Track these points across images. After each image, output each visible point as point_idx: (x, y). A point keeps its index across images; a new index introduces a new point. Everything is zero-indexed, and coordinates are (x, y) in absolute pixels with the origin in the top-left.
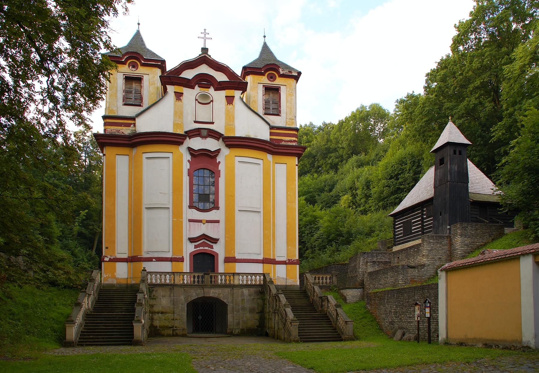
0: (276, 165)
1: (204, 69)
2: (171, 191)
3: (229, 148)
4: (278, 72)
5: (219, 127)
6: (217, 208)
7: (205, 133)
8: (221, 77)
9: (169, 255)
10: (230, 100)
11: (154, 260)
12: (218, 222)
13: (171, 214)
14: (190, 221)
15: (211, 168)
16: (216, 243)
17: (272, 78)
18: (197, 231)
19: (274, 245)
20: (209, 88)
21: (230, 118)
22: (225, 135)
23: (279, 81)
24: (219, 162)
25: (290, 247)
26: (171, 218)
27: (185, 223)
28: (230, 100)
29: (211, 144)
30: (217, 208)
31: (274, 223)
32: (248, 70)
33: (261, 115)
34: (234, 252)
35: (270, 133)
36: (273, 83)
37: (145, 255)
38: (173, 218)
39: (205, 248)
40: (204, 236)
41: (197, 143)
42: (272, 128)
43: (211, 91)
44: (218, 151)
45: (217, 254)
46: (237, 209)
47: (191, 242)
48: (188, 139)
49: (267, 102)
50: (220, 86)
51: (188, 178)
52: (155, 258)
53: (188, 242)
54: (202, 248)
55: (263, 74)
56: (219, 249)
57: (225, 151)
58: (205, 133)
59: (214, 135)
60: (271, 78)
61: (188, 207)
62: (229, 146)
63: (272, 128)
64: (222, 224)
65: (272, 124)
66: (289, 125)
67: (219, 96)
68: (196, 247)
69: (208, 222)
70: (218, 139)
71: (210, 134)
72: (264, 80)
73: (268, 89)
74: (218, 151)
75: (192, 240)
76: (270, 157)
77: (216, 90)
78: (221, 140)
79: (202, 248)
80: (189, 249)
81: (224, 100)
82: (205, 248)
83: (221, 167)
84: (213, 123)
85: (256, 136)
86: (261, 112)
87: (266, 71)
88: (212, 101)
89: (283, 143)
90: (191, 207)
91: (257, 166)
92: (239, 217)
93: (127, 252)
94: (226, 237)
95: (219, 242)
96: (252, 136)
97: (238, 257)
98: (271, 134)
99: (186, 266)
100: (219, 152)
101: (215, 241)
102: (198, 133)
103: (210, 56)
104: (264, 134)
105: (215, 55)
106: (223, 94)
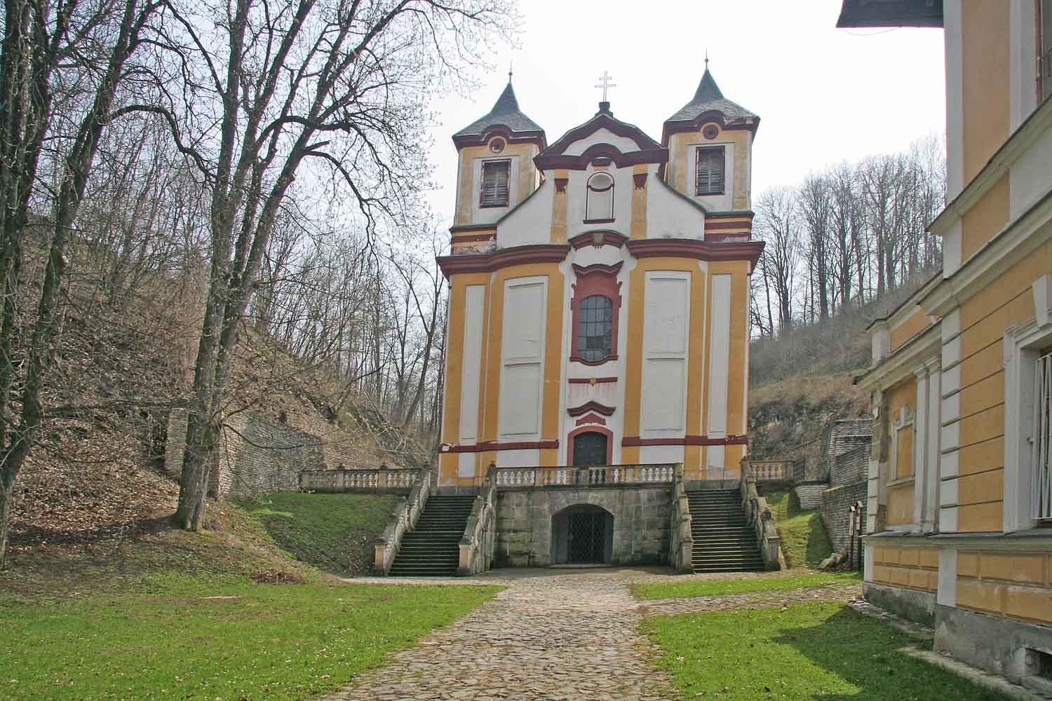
1: (602, 137)
3: (637, 258)
4: (722, 123)
5: (622, 226)
6: (615, 358)
7: (599, 238)
8: (627, 146)
10: (640, 181)
12: (614, 380)
14: (571, 381)
16: (610, 415)
17: (711, 134)
18: (581, 397)
20: (609, 165)
21: (639, 209)
22: (631, 239)
23: (722, 138)
24: (621, 283)
27: (564, 385)
28: (640, 181)
29: (608, 255)
30: (615, 358)
32: (671, 127)
33: (692, 196)
35: (705, 224)
36: (715, 141)
40: (592, 405)
41: (587, 256)
42: (708, 216)
43: (612, 169)
44: (619, 266)
46: (645, 356)
47: (572, 416)
48: (573, 250)
49: (701, 175)
50: (625, 161)
55: (697, 130)
56: (615, 426)
57: (631, 264)
58: (599, 238)
59: (614, 239)
60: (711, 133)
62: (636, 255)
63: (708, 216)
64: (621, 384)
65: (710, 210)
66: (738, 207)
67: (623, 176)
68: (578, 423)
69: (599, 381)
71: (607, 238)
72: (699, 138)
73: (704, 153)
74: (619, 266)
75: (573, 412)
76: (703, 266)
77: (620, 166)
78: (624, 246)
80: (568, 426)
83: (624, 292)
84: (612, 220)
85: (681, 234)
86: (691, 191)
87: (701, 124)
88: (613, 185)
89: (728, 240)
90: (573, 359)
91: (680, 284)
92: (649, 372)
94: (626, 405)
95: (614, 413)
96: (675, 236)
98: (707, 227)
99: (562, 456)
100: (621, 267)
101: (609, 411)
102: (589, 239)
103: (611, 114)
104: (695, 229)
105: (621, 113)
106: (630, 171)
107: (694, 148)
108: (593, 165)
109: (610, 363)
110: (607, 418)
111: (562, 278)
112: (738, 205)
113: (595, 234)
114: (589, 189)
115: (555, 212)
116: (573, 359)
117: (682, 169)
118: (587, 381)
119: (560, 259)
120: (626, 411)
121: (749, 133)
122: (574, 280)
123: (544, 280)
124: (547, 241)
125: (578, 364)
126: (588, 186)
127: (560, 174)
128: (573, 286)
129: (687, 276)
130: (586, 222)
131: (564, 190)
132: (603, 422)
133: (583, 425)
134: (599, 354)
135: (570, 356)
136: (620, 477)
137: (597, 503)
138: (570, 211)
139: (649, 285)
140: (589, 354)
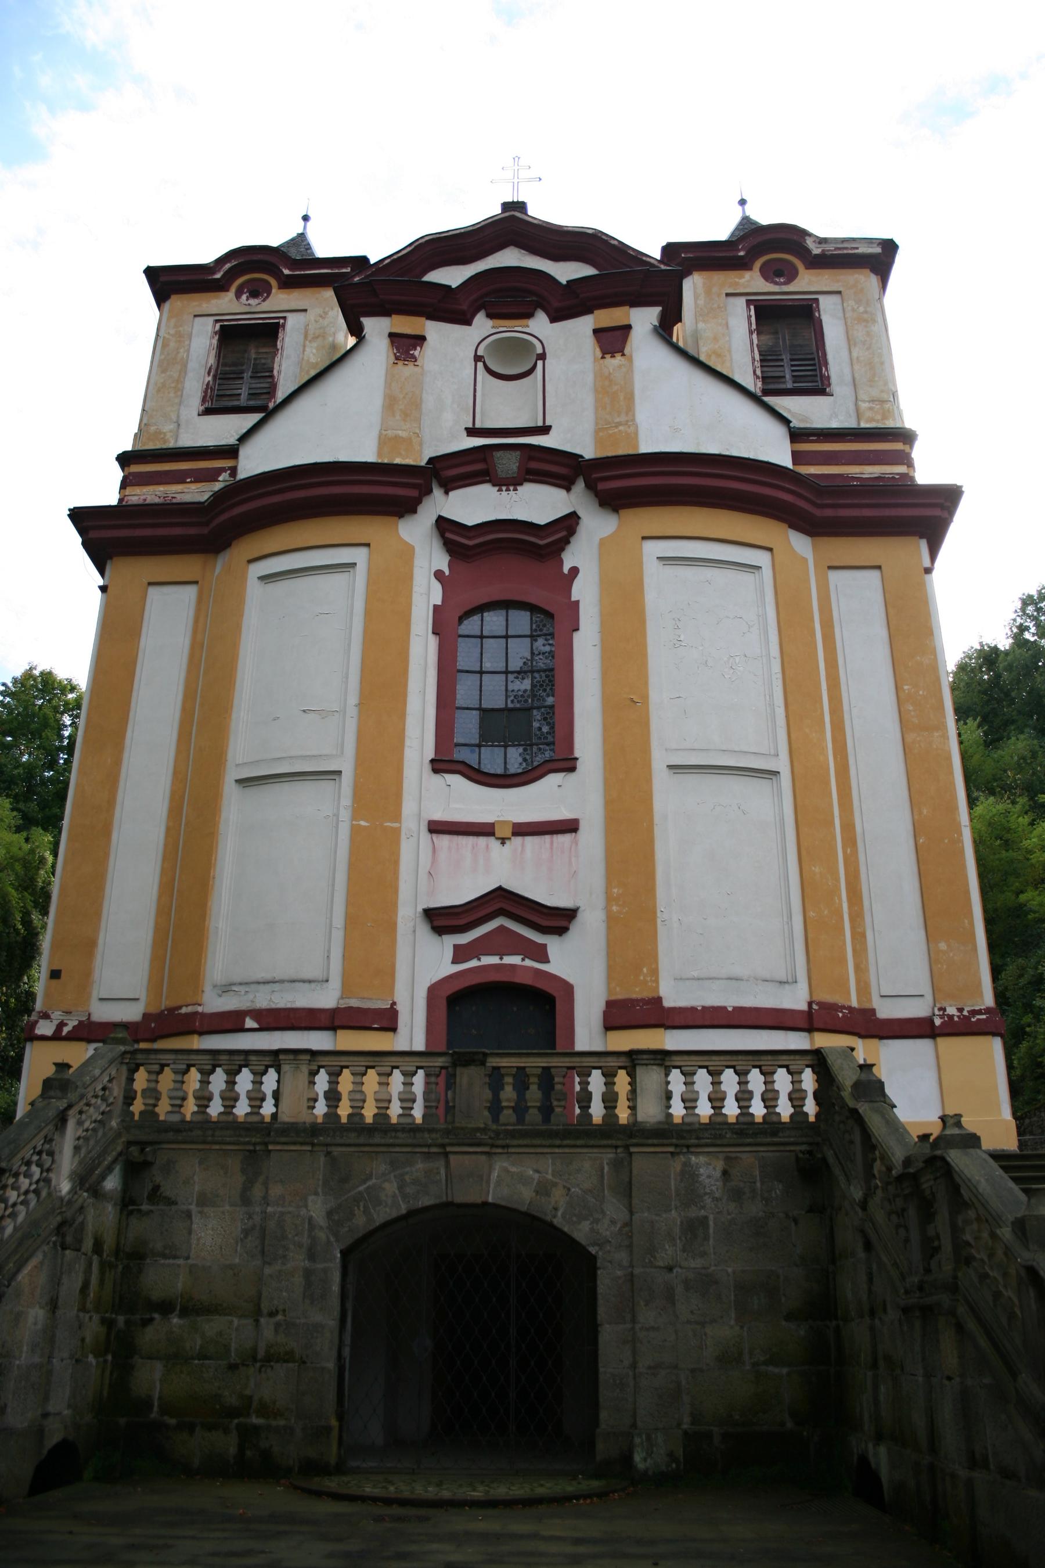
0: (834, 576)
2: (353, 699)
6: (568, 765)
9: (327, 998)
11: (250, 1023)
12: (570, 827)
13: (346, 800)
14: (437, 828)
15: (535, 597)
16: (561, 931)
17: (775, 272)
19: (859, 937)
20: (529, 315)
24: (574, 571)
25: (943, 946)
26: (345, 815)
30: (568, 765)
31: (849, 828)
34: (655, 972)
37: (214, 1003)
38: (356, 814)
39: (509, 960)
42: (797, 435)
43: (540, 325)
45: (568, 989)
46: (659, 760)
51: (433, 642)
52: (257, 1014)
53: (424, 931)
54: (494, 960)
58: (509, 463)
61: (427, 767)
65: (795, 423)
66: (867, 421)
68: (460, 954)
69: (522, 830)
70: (567, 485)
71: (534, 465)
72: (753, 281)
76: (800, 544)
77: (553, 319)
79: (494, 960)
81: (589, 345)
82: (509, 960)
84: (545, 430)
88: (542, 357)
90: (440, 765)
91: (747, 578)
93: (142, 993)
94: (609, 899)
95: (575, 928)
97: (673, 996)
102: (479, 467)
106: (584, 326)
107: (742, 301)
108: (490, 316)
109: (552, 780)
110: (553, 945)
111: (407, 553)
112: (869, 414)
113: (498, 454)
114: (480, 365)
115: (390, 403)
116: (440, 765)
117: (715, 339)
118: (484, 830)
119: (406, 508)
120: (611, 920)
121: (869, 280)
122: (442, 561)
123: (359, 556)
124: (367, 453)
125: (457, 781)
126: (478, 358)
127: (405, 325)
128: (439, 575)
129: (761, 558)
130: (472, 432)
131: (415, 359)
132: (541, 954)
133: (473, 963)
134: (515, 760)
135: (431, 755)
136: (610, 1100)
137: (524, 1196)
138: (429, 401)
139: (654, 575)
140: (492, 760)
